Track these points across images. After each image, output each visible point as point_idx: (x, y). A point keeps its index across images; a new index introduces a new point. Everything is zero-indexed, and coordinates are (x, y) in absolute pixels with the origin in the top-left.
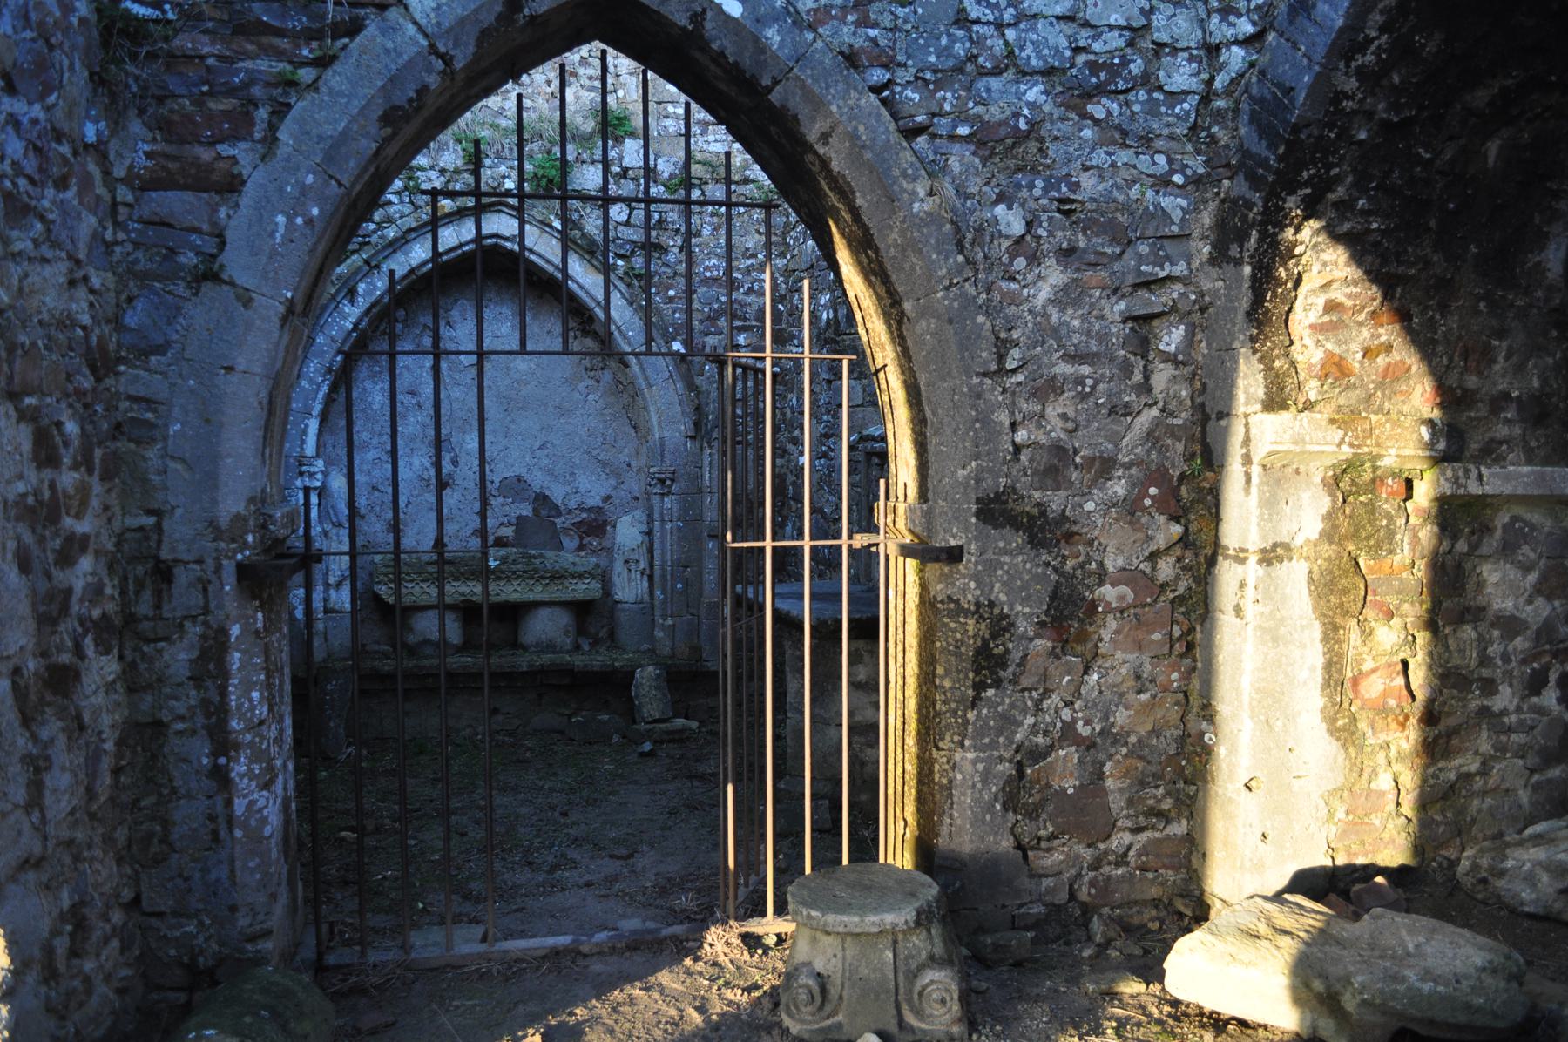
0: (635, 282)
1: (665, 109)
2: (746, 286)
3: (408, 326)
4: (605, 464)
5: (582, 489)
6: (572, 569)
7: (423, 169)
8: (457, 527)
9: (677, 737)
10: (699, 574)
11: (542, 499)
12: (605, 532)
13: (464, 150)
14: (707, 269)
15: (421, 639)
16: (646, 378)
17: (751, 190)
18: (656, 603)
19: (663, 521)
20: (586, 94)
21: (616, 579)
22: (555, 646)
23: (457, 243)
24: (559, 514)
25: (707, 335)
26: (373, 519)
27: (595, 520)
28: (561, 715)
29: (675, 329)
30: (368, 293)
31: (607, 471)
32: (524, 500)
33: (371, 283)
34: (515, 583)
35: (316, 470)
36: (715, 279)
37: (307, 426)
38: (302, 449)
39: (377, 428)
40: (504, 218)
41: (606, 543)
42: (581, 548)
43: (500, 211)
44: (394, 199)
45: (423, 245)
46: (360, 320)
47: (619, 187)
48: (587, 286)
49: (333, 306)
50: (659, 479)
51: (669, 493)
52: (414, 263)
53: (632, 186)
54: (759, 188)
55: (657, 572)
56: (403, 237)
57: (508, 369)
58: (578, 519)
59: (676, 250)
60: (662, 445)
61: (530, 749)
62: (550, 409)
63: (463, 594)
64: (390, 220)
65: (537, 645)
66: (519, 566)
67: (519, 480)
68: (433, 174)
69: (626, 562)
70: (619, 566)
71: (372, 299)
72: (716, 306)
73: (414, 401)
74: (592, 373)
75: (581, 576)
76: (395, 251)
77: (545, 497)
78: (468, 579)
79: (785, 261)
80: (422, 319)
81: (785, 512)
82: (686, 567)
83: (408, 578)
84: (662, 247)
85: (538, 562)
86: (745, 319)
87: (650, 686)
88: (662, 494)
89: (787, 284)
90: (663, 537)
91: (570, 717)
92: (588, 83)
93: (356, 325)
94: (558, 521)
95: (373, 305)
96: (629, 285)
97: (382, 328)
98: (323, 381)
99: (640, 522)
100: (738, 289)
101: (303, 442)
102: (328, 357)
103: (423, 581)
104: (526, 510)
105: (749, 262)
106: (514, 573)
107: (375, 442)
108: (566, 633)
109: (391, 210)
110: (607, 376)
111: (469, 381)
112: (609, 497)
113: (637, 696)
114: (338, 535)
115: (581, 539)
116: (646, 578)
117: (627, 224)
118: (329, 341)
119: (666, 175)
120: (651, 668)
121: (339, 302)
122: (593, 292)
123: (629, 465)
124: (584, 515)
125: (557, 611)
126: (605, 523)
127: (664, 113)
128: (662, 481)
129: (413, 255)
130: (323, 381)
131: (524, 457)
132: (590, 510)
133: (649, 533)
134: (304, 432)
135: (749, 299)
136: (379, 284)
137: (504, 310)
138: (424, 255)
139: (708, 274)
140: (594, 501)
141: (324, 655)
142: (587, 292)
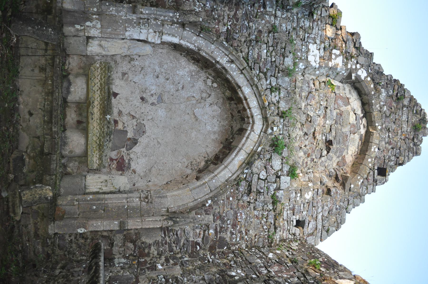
0: (236, 183)
1: (299, 193)
2: (234, 232)
3: (210, 88)
4: (150, 170)
5: (139, 160)
7: (279, 94)
8: (123, 104)
9: (11, 210)
10: (100, 218)
11: (135, 142)
12: (118, 170)
13: (287, 111)
14: (241, 214)
15: (71, 81)
16: (194, 189)
17: (272, 231)
18: (86, 196)
19: (127, 198)
20: (302, 161)
21: (97, 176)
22: (64, 146)
23: (251, 106)
25: (214, 215)
26: (129, 67)
27: (124, 166)
28: (27, 148)
29: (216, 201)
30: (231, 68)
31: (147, 171)
32: (135, 134)
33: (235, 70)
34: (98, 128)
36: (237, 218)
37: (176, 37)
38: (166, 34)
39: (168, 72)
40: (261, 127)
41: (114, 171)
42: (112, 160)
43: (263, 125)
44: (268, 82)
45: (250, 92)
46: (220, 64)
47: (273, 175)
48: (234, 161)
49: (227, 53)
50: (148, 195)
52: (243, 89)
53: (274, 180)
54: (273, 234)
55: (102, 196)
57: (192, 129)
58: (125, 158)
59: (249, 200)
60: (164, 197)
61: (8, 129)
63: (93, 102)
64: (259, 80)
65: (66, 137)
66: (106, 129)
67: (144, 132)
68: (277, 98)
70: (104, 177)
71: (229, 70)
72: (226, 219)
73: (180, 88)
74: (190, 165)
75: (100, 159)
76: (248, 81)
77: (136, 144)
79: (244, 248)
80: (213, 93)
81: (131, 257)
82: (104, 211)
83: (102, 77)
84: (250, 194)
85: (108, 138)
86: (220, 232)
87: (41, 194)
88: (140, 198)
89: (235, 250)
90: (119, 199)
91: (26, 152)
92: (305, 161)
93: (218, 62)
94: (124, 149)
95: (226, 70)
96: (235, 180)
97: (210, 77)
98: (195, 46)
99: (125, 187)
100: (233, 228)
101: (169, 35)
102: (205, 49)
103: (101, 84)
104: (130, 135)
105: (244, 232)
106: (103, 127)
107: (163, 70)
108: (71, 152)
109: (264, 80)
110: (189, 171)
111: (187, 112)
113: (36, 187)
114: (125, 47)
115: (116, 160)
116: (98, 190)
117: (259, 178)
118: (212, 50)
119: (278, 194)
120: (51, 194)
121: (228, 56)
122: (231, 164)
123: (150, 181)
124: (127, 161)
125: (83, 148)
126: (123, 171)
127: (297, 192)
128: (147, 198)
129: (246, 88)
130: (195, 46)
131: (154, 134)
132: (129, 164)
133: (119, 192)
134: (173, 36)
135: (228, 233)
136: (235, 73)
137: (216, 128)
138: (246, 93)
139: (239, 215)
140: (133, 166)
141: (66, 34)
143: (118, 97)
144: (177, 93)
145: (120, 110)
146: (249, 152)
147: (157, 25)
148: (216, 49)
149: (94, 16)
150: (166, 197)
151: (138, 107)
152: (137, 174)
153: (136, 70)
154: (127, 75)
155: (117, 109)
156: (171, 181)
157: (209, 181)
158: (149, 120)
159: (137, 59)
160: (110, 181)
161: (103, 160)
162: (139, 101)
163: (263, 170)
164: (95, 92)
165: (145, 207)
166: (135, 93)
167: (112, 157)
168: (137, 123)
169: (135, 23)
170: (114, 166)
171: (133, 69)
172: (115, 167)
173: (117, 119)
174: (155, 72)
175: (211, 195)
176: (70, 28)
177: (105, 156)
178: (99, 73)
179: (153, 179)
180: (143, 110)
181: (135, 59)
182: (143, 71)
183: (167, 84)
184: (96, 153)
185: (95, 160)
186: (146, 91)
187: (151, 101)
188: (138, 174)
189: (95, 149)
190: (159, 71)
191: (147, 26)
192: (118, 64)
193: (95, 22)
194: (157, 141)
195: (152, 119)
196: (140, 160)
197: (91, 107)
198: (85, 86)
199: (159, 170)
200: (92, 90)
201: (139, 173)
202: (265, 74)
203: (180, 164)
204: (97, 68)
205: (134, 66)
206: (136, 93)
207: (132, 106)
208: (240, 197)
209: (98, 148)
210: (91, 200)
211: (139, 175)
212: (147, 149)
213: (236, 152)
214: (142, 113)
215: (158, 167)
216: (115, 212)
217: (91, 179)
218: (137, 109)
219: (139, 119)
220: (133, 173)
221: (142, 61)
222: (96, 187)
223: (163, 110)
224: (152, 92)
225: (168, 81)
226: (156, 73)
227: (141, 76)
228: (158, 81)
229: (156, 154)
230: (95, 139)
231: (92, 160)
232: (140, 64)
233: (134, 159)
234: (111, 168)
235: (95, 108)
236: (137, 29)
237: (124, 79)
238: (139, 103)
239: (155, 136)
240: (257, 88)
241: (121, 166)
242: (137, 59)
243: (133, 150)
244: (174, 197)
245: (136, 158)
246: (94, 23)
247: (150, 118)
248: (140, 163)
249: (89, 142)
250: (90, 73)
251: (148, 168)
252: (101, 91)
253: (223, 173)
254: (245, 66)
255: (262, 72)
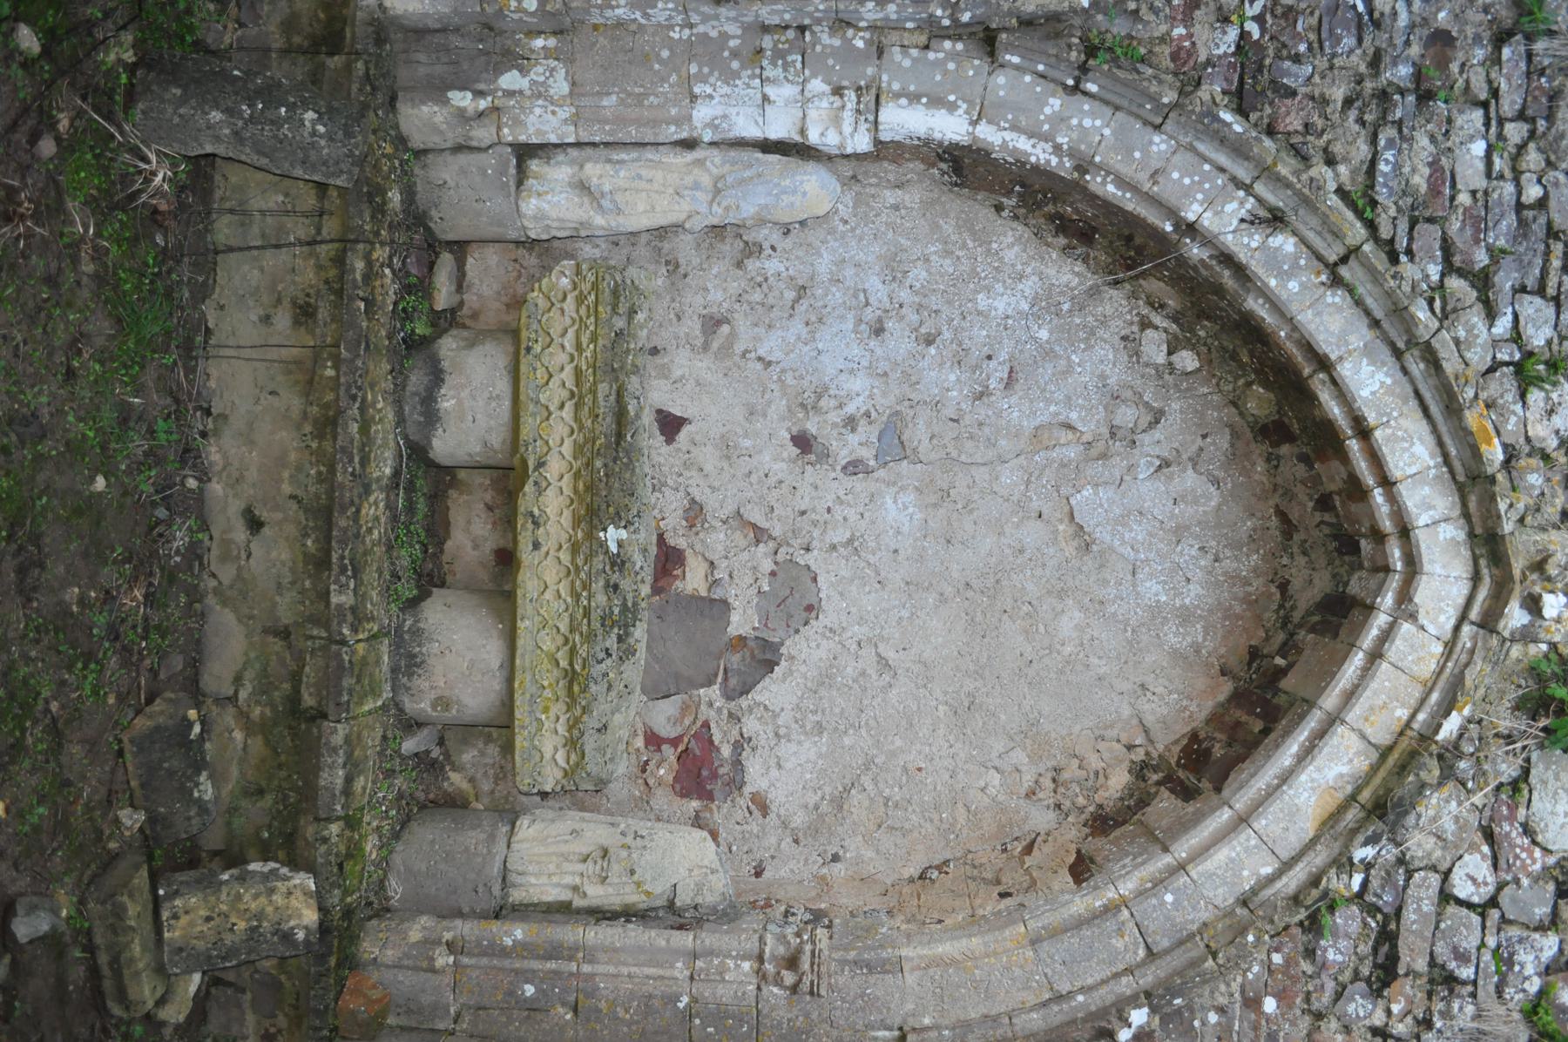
0: (1302, 914)
3: (1160, 376)
4: (839, 802)
5: (786, 749)
6: (591, 722)
8: (708, 468)
9: (108, 985)
11: (765, 658)
12: (685, 794)
15: (445, 364)
16: (1055, 933)
19: (695, 956)
22: (410, 675)
24: (729, 696)
26: (734, 287)
27: (714, 776)
28: (238, 680)
29: (1179, 1011)
30: (1273, 259)
32: (766, 620)
33: (1295, 266)
35: (847, 128)
37: (952, 108)
38: (898, 96)
39: (934, 302)
40: (1460, 591)
41: (663, 799)
43: (1476, 579)
44: (1503, 325)
45: (1389, 391)
46: (1207, 240)
47: (1536, 879)
48: (1289, 792)
49: (1243, 174)
51: (760, 974)
52: (1345, 370)
53: (1541, 911)
55: (570, 933)
56: (1412, 342)
57: (1061, 594)
58: (717, 738)
59: (1378, 1019)
62: (970, 685)
63: (541, 464)
64: (1446, 316)
65: (417, 632)
67: (810, 608)
69: (605, 853)
70: (597, 832)
71: (1256, 266)
73: (993, 384)
74: (1047, 783)
76: (1375, 324)
77: (770, 665)
78: (577, 476)
80: (1175, 406)
82: (575, 1010)
83: (585, 340)
87: (259, 916)
88: (760, 959)
93: (1191, 229)
94: (714, 692)
95: (1240, 270)
96: (1296, 900)
97: (1157, 319)
98: (1057, 149)
99: (699, 887)
101: (914, 98)
102: (1116, 161)
103: (578, 373)
104: (741, 622)
106: (586, 586)
107: (904, 295)
108: (442, 702)
109: (1476, 318)
110: (1041, 819)
111: (1036, 504)
112: (764, 809)
113: (242, 879)
114: (696, 186)
115: (674, 742)
116: (565, 896)
117: (1446, 897)
118: (1155, 164)
121: (1248, 189)
122: (1275, 808)
123: (836, 858)
124: (726, 751)
125: (497, 685)
128: (792, 962)
129: (1366, 368)
130: (1057, 149)
131: (861, 621)
132: (738, 764)
134: (937, 102)
136: (1293, 286)
137: (1195, 589)
138: (1365, 393)
140: (757, 775)
141: (417, 141)
142: (1272, 792)
143: (683, 435)
144: (982, 411)
145: (693, 501)
146: (1382, 737)
147: (847, 54)
148: (1177, 158)
149: (539, 43)
150: (898, 966)
151: (781, 482)
152: (773, 816)
153: (771, 301)
154: (725, 329)
155: (682, 494)
156: (942, 867)
157: (1141, 893)
158: (833, 547)
159: (773, 248)
160: (624, 853)
161: (588, 749)
162: (785, 455)
163: (1473, 848)
164: (550, 414)
165: (782, 1014)
166: (765, 415)
167: (656, 730)
168: (776, 563)
169: (735, 54)
170: (662, 772)
171: (757, 296)
172: (670, 778)
173: (679, 542)
174: (867, 304)
175: (1148, 978)
176: (425, 109)
177: (599, 730)
178: (568, 321)
179: (854, 847)
180: (807, 499)
181: (766, 245)
182: (803, 306)
183: (925, 364)
184: (552, 714)
185: (548, 751)
186: (823, 403)
187: (844, 452)
188: (779, 816)
189: (548, 693)
190: (886, 299)
191: (799, 65)
192: (685, 276)
193: (540, 69)
194: (879, 655)
195: (850, 541)
196: (793, 747)
197: (529, 488)
198: (503, 386)
199: (886, 805)
200: (538, 402)
201: (782, 812)
202: (1482, 281)
203: (995, 779)
204: (560, 296)
205: (759, 279)
206: (773, 413)
207: (754, 478)
208: (1327, 997)
209: (562, 693)
210: (523, 950)
211: (785, 825)
212: (823, 692)
213: (1303, 735)
214: (803, 513)
215: (881, 785)
216: (629, 1024)
217: (534, 839)
218: (775, 493)
219: (788, 544)
220: (756, 813)
221: (800, 253)
222: (555, 879)
223: (909, 497)
224: (850, 409)
225: (932, 350)
226: (870, 309)
227: (797, 327)
228: (879, 352)
229: (872, 722)
230: (548, 645)
231: (535, 747)
232: (791, 272)
233: (763, 742)
234: (651, 782)
235: (550, 492)
236: (748, 86)
237: (715, 345)
238: (784, 465)
239: (865, 629)
240: (1432, 360)
241: (699, 775)
242: (773, 248)
243: (758, 698)
244: (936, 972)
245: (771, 735)
246: (538, 73)
247: (839, 535)
248: (788, 765)
249: (518, 662)
250: (523, 320)
251: (828, 790)
252: (577, 407)
253: (1222, 855)
254: (1351, 241)
255: (1461, 273)
